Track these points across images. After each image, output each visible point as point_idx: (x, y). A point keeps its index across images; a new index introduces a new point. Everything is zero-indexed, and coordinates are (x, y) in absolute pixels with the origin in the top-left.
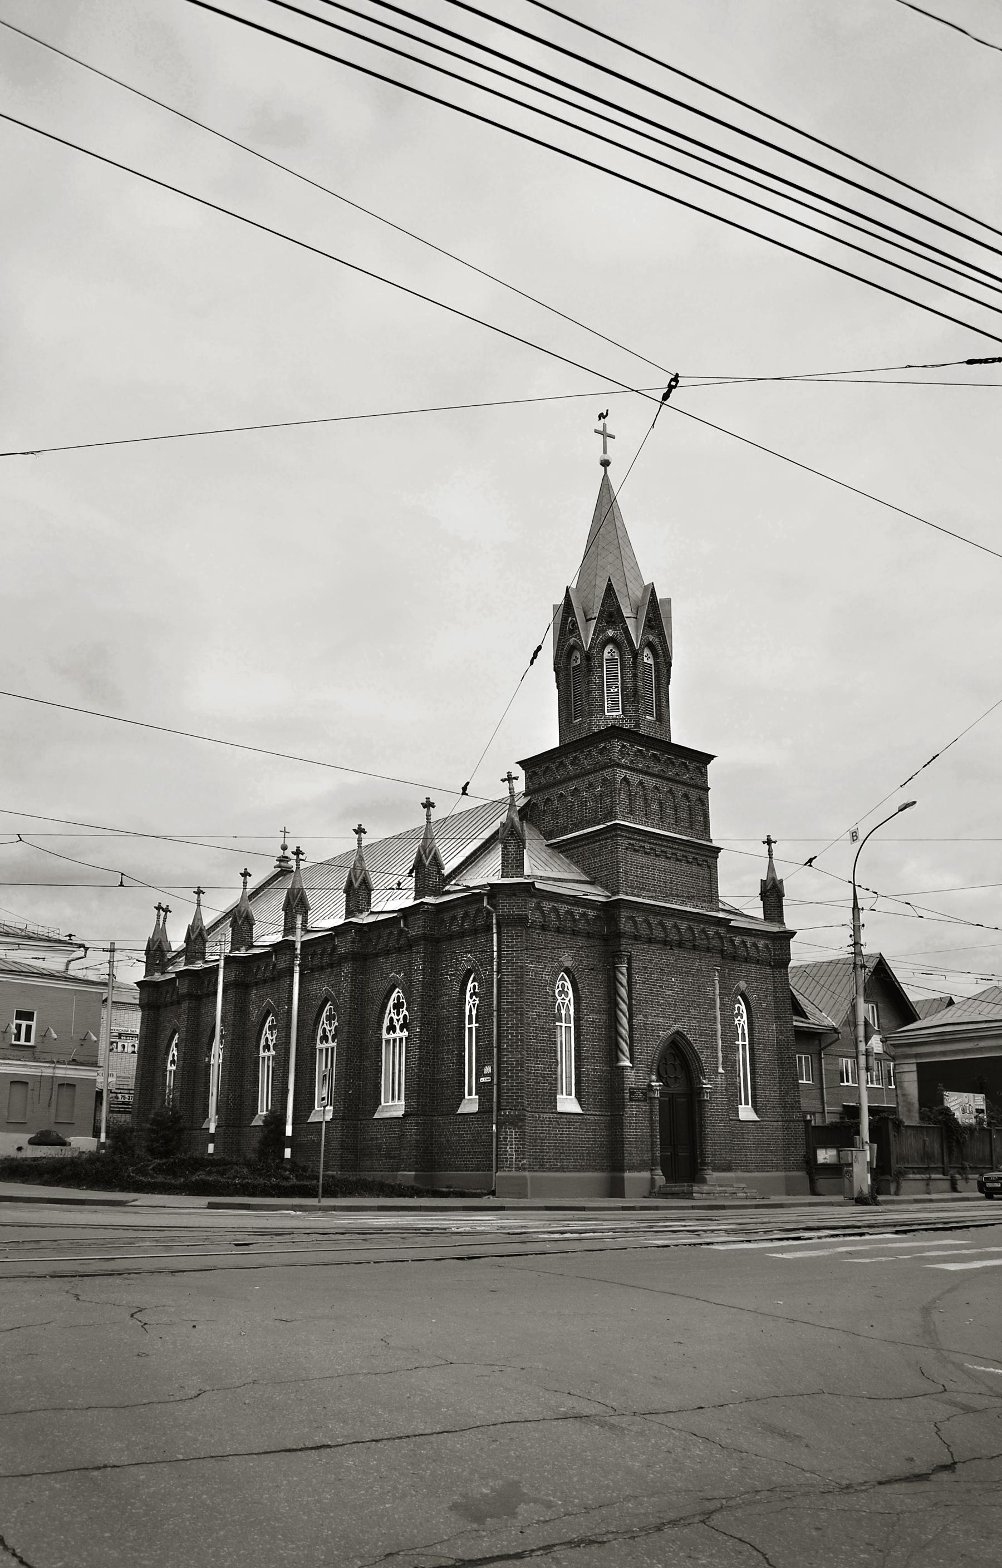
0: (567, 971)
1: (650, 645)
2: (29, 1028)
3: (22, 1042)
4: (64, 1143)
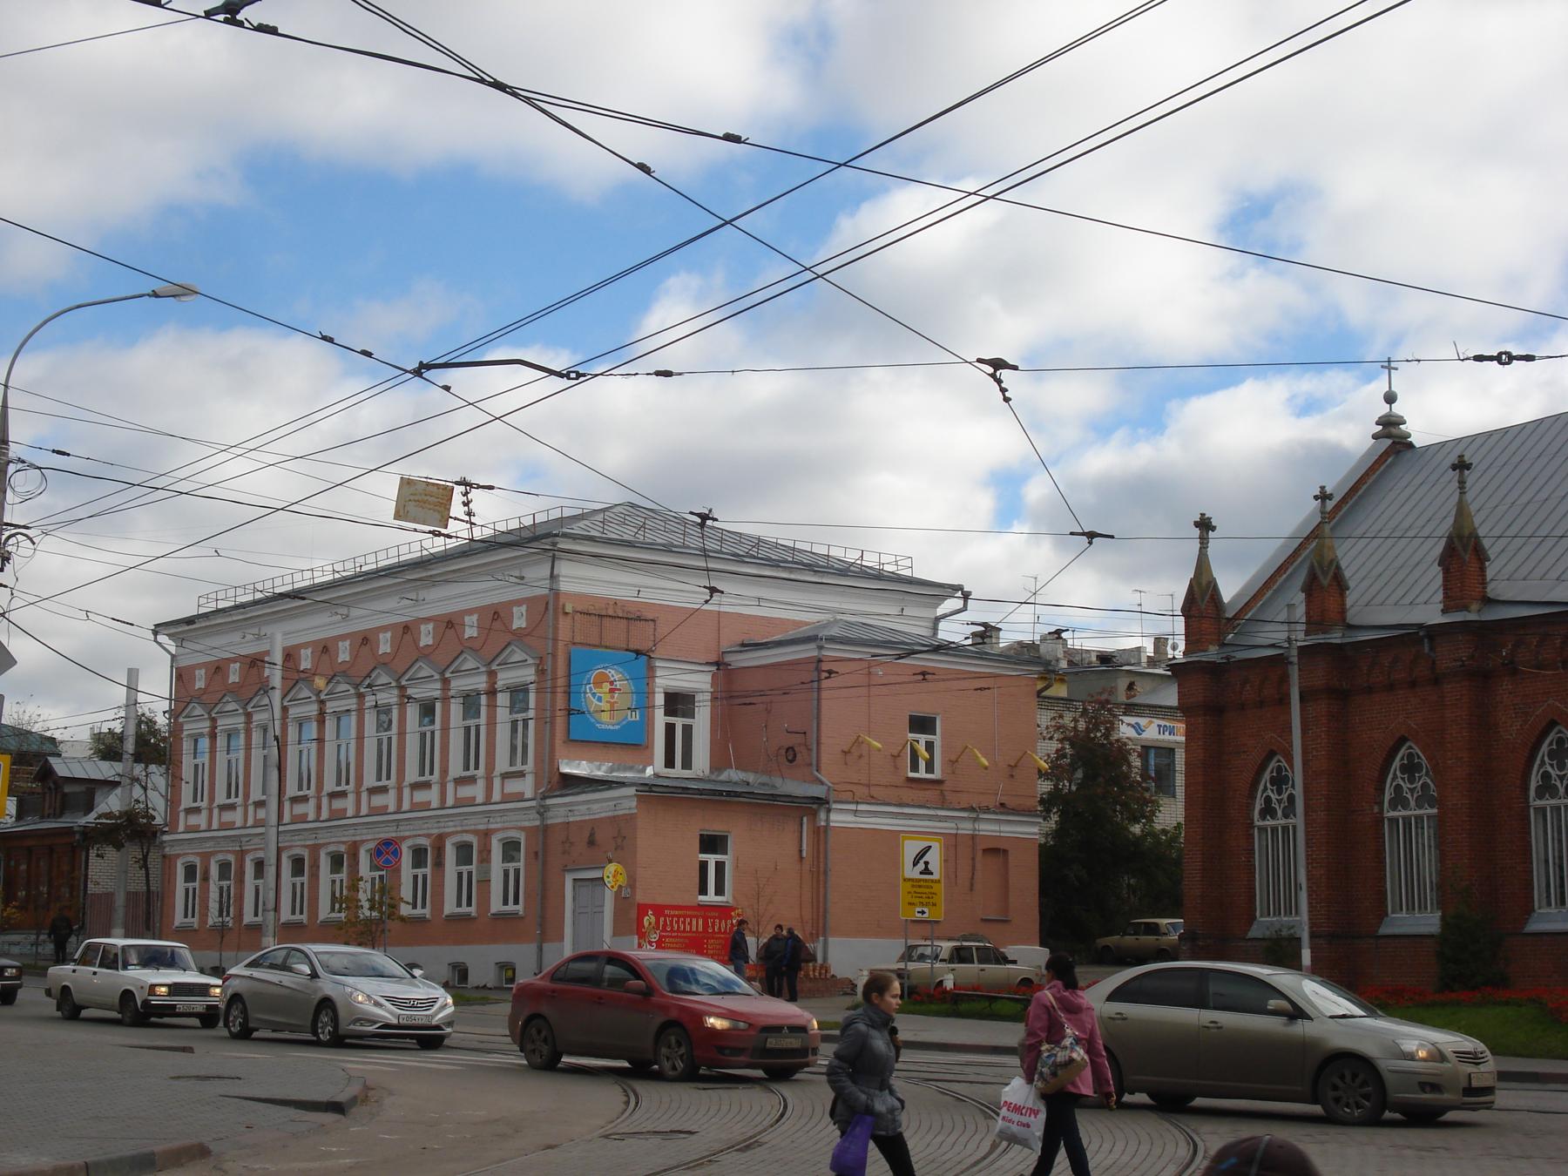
2: (930, 746)
3: (922, 774)
4: (1006, 960)
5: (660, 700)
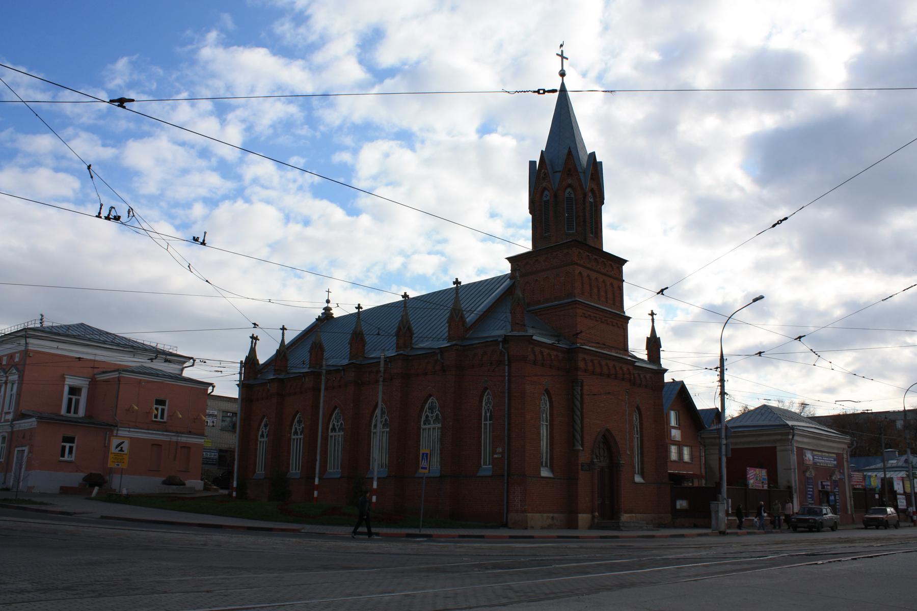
0: (547, 391)
1: (592, 190)
2: (163, 410)
3: (159, 419)
5: (66, 389)
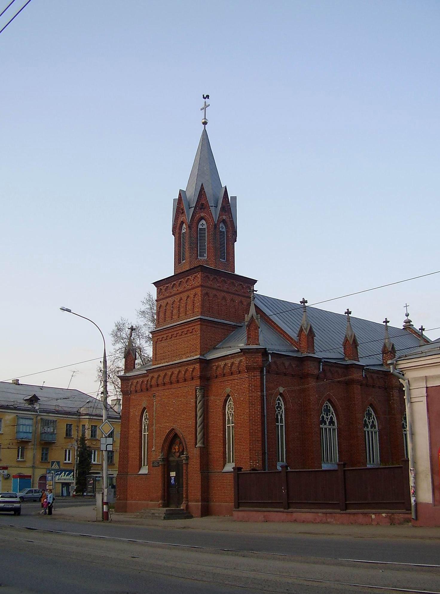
1: (224, 221)
